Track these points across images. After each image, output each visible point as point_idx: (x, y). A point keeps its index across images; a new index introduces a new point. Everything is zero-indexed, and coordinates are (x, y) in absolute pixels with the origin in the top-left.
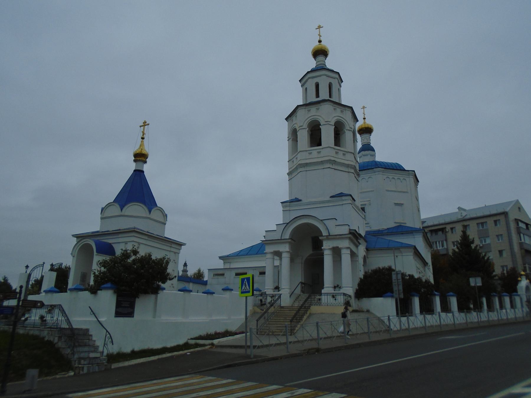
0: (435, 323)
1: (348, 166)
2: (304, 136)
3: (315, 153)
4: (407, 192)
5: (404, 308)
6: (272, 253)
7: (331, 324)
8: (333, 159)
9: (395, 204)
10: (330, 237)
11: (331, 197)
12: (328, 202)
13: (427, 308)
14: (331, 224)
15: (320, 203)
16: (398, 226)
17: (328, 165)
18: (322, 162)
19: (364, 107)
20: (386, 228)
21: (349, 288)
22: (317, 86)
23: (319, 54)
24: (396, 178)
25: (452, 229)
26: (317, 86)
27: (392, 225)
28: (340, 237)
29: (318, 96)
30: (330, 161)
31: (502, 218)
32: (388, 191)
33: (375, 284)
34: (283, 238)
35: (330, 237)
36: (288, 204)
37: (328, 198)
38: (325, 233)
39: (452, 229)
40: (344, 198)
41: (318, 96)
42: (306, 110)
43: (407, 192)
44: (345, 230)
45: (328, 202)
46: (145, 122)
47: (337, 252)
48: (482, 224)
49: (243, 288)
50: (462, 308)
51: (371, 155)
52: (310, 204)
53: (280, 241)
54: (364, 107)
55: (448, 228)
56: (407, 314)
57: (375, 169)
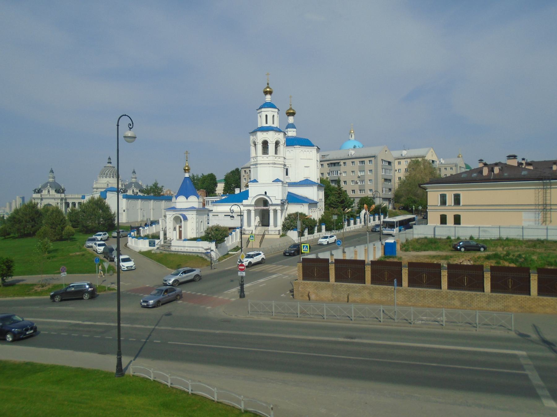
1: (281, 164)
2: (260, 147)
5: (301, 234)
10: (272, 205)
13: (311, 232)
17: (271, 165)
19: (291, 97)
21: (280, 227)
22: (266, 116)
25: (344, 163)
26: (266, 116)
27: (302, 179)
28: (277, 205)
29: (267, 123)
31: (373, 159)
33: (290, 223)
35: (272, 205)
38: (270, 203)
41: (267, 123)
47: (275, 211)
48: (362, 162)
50: (327, 229)
54: (291, 97)
55: (342, 163)
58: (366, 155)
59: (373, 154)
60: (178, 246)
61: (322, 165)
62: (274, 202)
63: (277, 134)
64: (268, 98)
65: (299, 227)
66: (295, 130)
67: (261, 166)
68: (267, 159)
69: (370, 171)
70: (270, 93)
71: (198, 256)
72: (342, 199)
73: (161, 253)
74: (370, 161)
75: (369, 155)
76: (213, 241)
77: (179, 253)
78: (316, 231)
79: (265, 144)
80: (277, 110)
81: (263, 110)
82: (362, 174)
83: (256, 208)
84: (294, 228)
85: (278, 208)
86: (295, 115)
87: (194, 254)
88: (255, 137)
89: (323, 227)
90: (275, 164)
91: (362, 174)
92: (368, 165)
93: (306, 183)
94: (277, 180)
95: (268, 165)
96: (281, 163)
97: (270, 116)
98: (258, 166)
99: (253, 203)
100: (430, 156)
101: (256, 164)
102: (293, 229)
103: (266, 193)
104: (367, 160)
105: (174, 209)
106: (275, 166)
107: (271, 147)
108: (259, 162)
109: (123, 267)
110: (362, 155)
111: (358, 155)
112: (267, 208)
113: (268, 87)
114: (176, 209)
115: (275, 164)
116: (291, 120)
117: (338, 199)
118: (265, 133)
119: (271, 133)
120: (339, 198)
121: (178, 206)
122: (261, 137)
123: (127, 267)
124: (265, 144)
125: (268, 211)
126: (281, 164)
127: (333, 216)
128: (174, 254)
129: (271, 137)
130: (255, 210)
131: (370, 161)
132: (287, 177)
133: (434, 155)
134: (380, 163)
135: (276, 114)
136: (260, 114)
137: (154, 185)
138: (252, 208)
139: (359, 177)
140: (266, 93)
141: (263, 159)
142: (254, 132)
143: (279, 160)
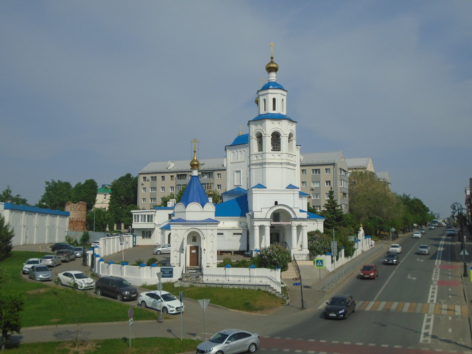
2: (268, 141)
10: (296, 219)
11: (287, 188)
12: (284, 191)
17: (284, 166)
18: (281, 163)
22: (274, 100)
26: (274, 100)
29: (274, 109)
31: (331, 167)
35: (296, 219)
36: (257, 189)
38: (293, 217)
40: (295, 189)
41: (274, 109)
45: (284, 191)
46: (195, 139)
48: (316, 170)
49: (318, 264)
53: (265, 220)
58: (321, 162)
59: (331, 161)
60: (213, 276)
61: (303, 171)
63: (290, 124)
64: (273, 77)
65: (334, 249)
67: (270, 166)
68: (278, 157)
69: (327, 182)
70: (275, 70)
71: (259, 290)
72: (339, 215)
73: (192, 286)
74: (326, 169)
75: (326, 162)
76: (278, 268)
77: (224, 286)
79: (276, 137)
80: (285, 93)
81: (270, 91)
82: (317, 185)
83: (273, 223)
87: (252, 288)
88: (259, 127)
90: (288, 164)
91: (317, 185)
92: (324, 176)
94: (291, 187)
95: (280, 166)
97: (278, 100)
98: (267, 166)
99: (269, 216)
100: (370, 169)
101: (265, 163)
102: (325, 253)
103: (276, 203)
104: (323, 169)
105: (182, 222)
107: (284, 141)
108: (267, 161)
109: (170, 309)
110: (315, 162)
111: (310, 162)
112: (288, 223)
113: (272, 62)
114: (186, 221)
115: (288, 164)
117: (332, 216)
118: (276, 123)
119: (285, 122)
120: (333, 214)
121: (189, 217)
122: (270, 127)
123: (177, 308)
124: (276, 137)
128: (217, 288)
129: (285, 128)
131: (326, 169)
133: (372, 167)
134: (339, 171)
135: (285, 98)
136: (265, 97)
137: (4, 193)
139: (312, 190)
140: (270, 69)
142: (261, 119)
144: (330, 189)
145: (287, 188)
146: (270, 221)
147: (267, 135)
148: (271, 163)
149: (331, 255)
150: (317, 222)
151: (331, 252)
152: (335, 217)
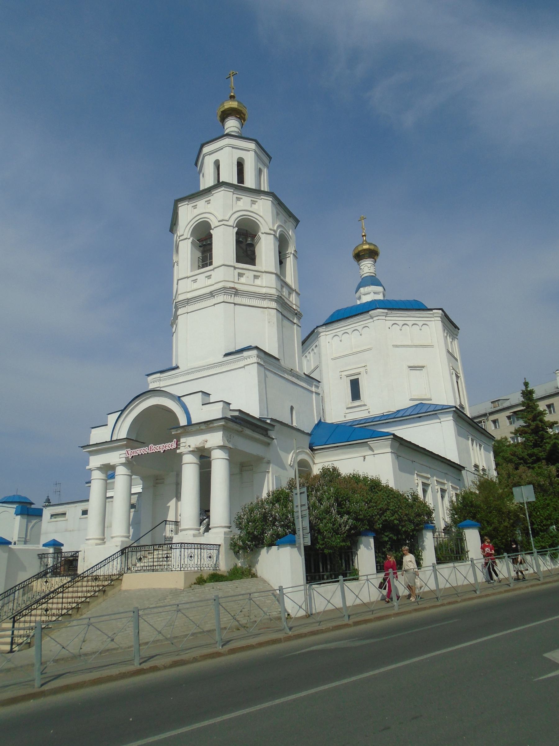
0: (461, 582)
1: (264, 297)
3: (201, 278)
4: (432, 346)
6: (98, 469)
7: (250, 599)
8: (232, 285)
9: (409, 367)
11: (227, 355)
12: (221, 364)
14: (194, 404)
15: (208, 369)
16: (417, 405)
17: (221, 298)
18: (212, 294)
20: (395, 410)
22: (217, 165)
23: (227, 117)
24: (410, 323)
26: (217, 165)
28: (207, 426)
30: (225, 290)
32: (397, 346)
34: (114, 438)
35: (192, 428)
37: (221, 358)
38: (183, 421)
39: (549, 406)
40: (245, 354)
42: (190, 206)
43: (432, 346)
44: (214, 412)
45: (221, 364)
47: (204, 458)
51: (375, 293)
52: (192, 372)
56: (341, 578)
57: (371, 313)
62: (200, 414)
66: (380, 289)
67: (190, 308)
68: (210, 282)
72: (548, 447)
78: (429, 555)
84: (284, 535)
85: (215, 439)
86: (379, 259)
89: (472, 538)
90: (236, 292)
93: (423, 412)
96: (264, 291)
106: (238, 300)
115: (236, 292)
116: (367, 267)
120: (535, 445)
125: (173, 460)
126: (264, 297)
127: (516, 490)
130: (129, 464)
132: (357, 403)
138: (116, 458)
141: (195, 286)
143: (258, 282)
144: (524, 388)
145: (227, 355)
146: (126, 446)
147: (181, 238)
148: (188, 301)
149: (292, 543)
150: (371, 449)
151: (294, 532)
152: (543, 455)
